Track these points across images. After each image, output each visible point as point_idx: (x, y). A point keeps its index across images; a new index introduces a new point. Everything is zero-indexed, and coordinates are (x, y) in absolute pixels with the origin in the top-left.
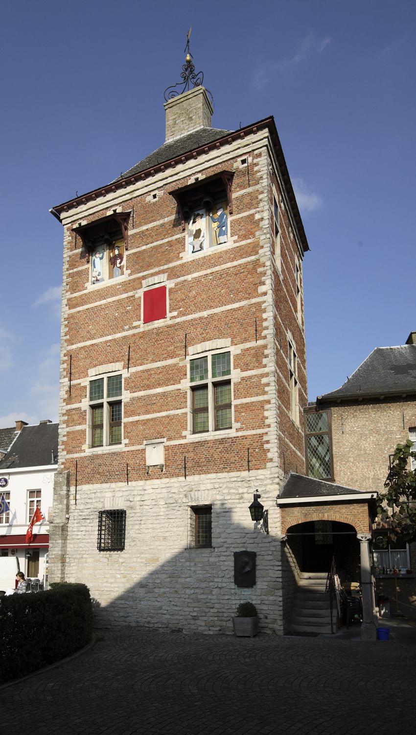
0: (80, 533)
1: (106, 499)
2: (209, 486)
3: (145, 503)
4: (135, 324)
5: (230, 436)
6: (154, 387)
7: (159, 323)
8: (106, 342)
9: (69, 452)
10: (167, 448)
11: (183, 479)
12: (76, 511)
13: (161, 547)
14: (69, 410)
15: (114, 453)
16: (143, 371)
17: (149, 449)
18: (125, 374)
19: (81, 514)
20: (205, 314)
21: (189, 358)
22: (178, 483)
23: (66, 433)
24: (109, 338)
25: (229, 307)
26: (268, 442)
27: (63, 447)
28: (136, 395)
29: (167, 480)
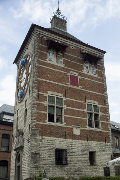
0: (45, 157)
1: (57, 144)
2: (95, 145)
3: (73, 148)
4: (67, 83)
5: (100, 131)
6: (75, 108)
7: (76, 87)
10: (81, 130)
11: (86, 141)
12: (42, 147)
13: (81, 165)
14: (38, 103)
15: (60, 127)
16: (71, 101)
17: (74, 129)
18: (64, 99)
19: (44, 148)
20: (91, 92)
21: (86, 103)
22: (84, 142)
23: (36, 112)
24: (57, 83)
25: (97, 93)
26: (110, 135)
28: (68, 108)
29: (81, 141)
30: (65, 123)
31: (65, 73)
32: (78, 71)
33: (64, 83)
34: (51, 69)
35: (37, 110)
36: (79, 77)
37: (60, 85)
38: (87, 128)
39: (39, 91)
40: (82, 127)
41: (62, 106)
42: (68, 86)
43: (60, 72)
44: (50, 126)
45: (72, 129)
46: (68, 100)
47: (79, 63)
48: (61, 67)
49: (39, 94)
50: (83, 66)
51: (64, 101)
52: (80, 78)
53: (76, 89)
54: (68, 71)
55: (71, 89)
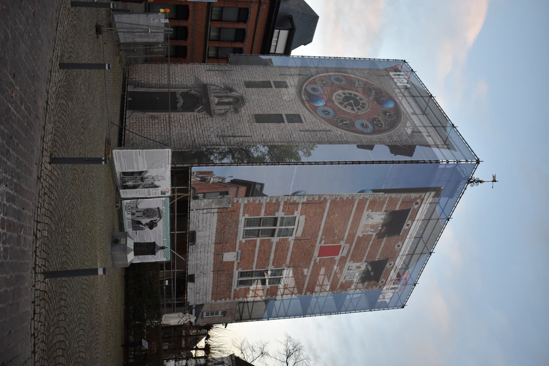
4: (323, 242)
7: (316, 253)
8: (320, 226)
9: (245, 205)
10: (233, 263)
17: (235, 254)
18: (291, 239)
24: (322, 227)
26: (226, 299)
27: (251, 201)
30: (244, 241)
31: (345, 238)
32: (350, 255)
33: (324, 237)
34: (351, 218)
35: (267, 203)
36: (337, 258)
37: (319, 231)
38: (237, 269)
39: (303, 203)
40: (238, 263)
41: (278, 236)
42: (318, 243)
43: (345, 231)
44: (237, 222)
45: (235, 251)
46: (289, 244)
47: (366, 256)
48: (356, 232)
49: (298, 204)
50: (361, 261)
51: (288, 239)
52: (336, 259)
53: (313, 254)
54: (350, 241)
55: (313, 246)
